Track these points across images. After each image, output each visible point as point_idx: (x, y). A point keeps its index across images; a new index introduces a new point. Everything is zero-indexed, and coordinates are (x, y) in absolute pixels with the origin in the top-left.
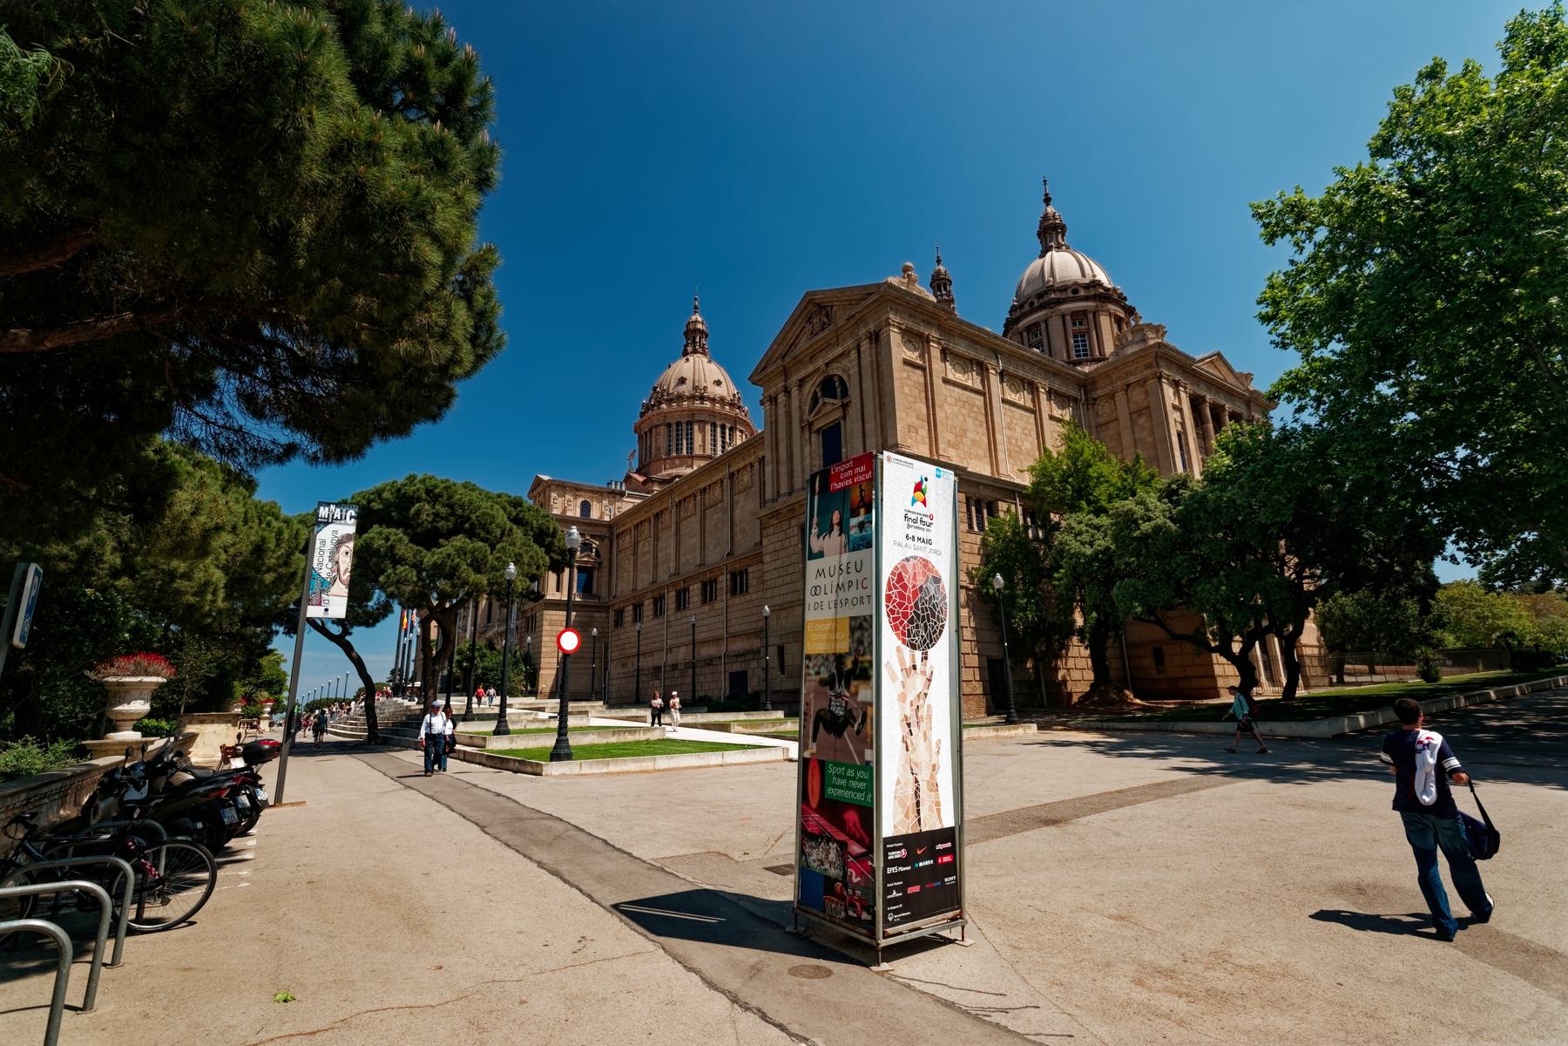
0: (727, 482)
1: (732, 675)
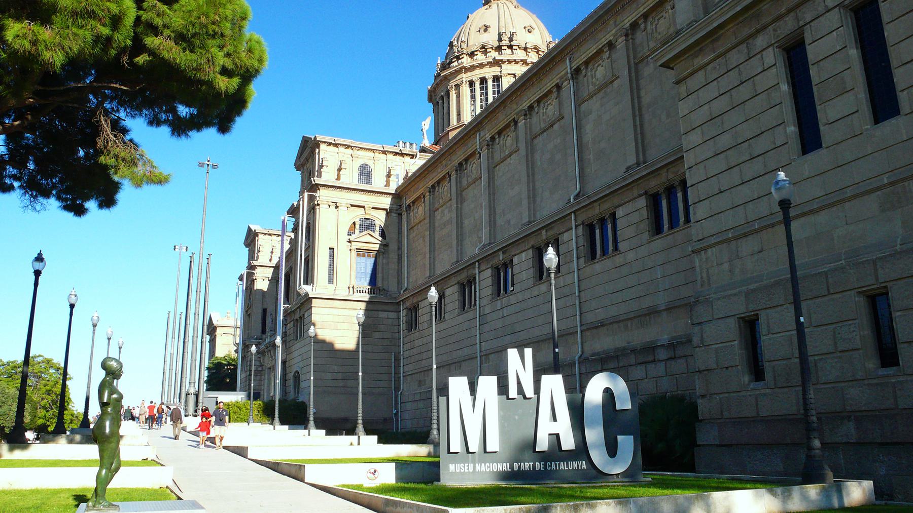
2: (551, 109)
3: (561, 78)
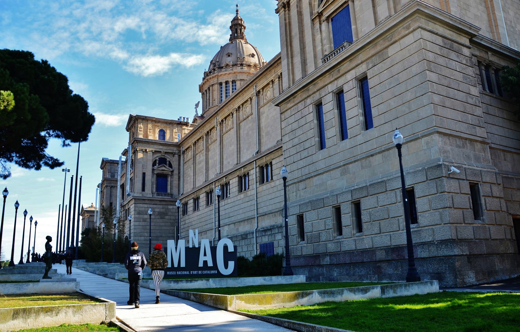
0: (255, 99)
1: (261, 246)
2: (247, 109)
3: (252, 95)
